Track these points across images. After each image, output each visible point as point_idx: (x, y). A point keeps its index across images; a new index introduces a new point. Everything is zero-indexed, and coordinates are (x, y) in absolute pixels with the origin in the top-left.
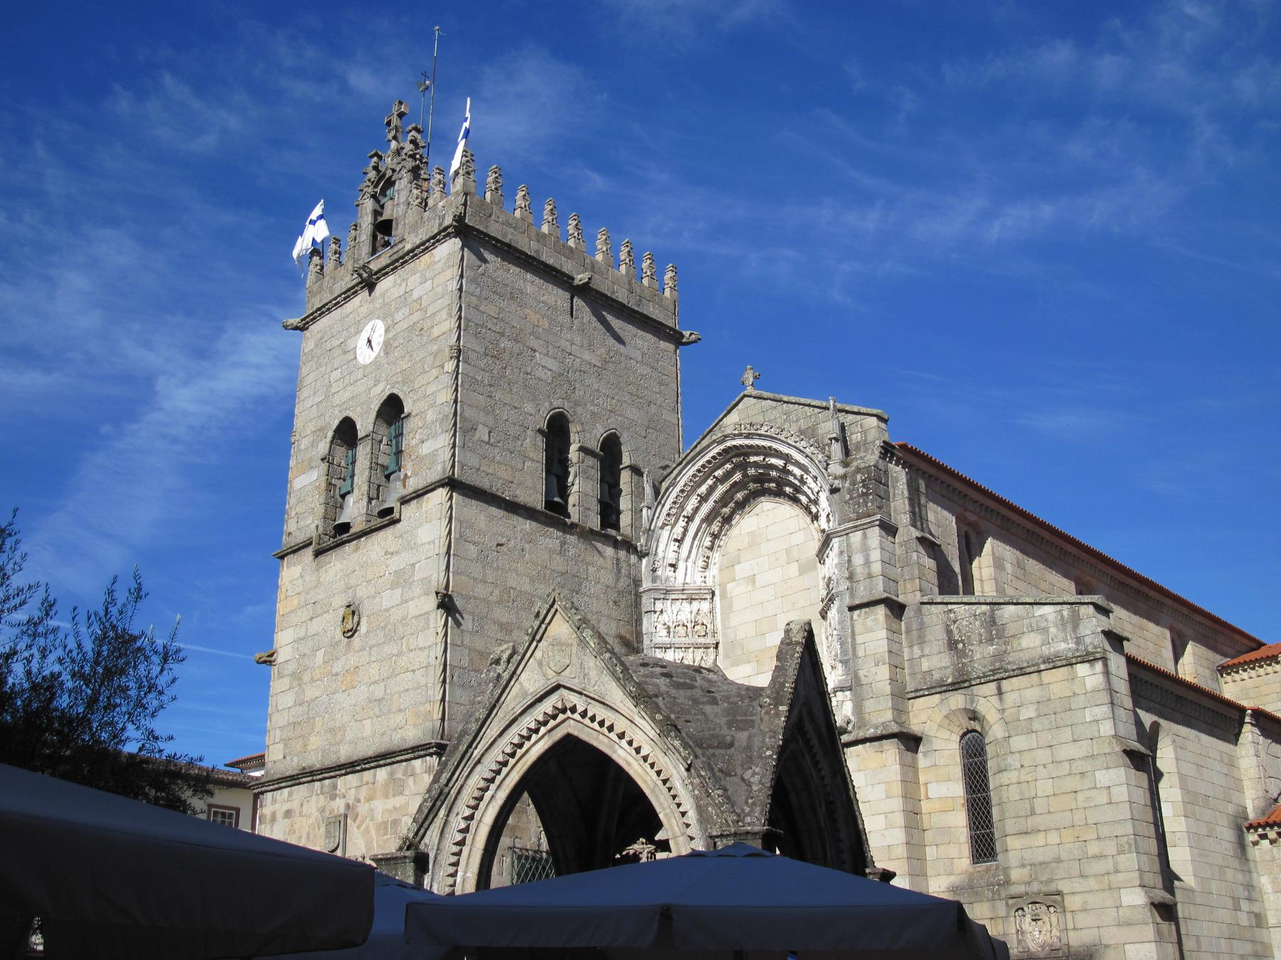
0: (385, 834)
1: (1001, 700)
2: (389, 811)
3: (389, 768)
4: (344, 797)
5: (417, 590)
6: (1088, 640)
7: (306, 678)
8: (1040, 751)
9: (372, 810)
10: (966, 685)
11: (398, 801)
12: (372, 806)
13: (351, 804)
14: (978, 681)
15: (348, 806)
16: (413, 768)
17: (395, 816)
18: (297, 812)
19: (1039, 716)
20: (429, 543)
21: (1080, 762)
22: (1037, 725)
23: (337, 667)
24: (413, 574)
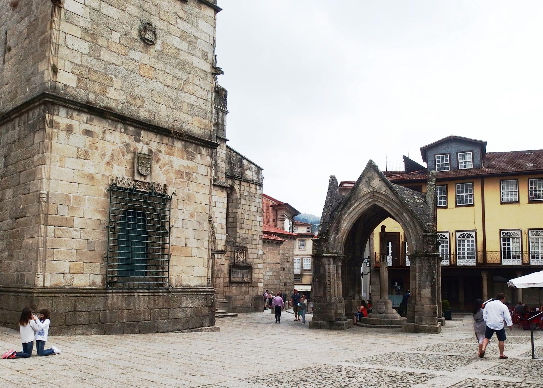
0: (182, 178)
1: (240, 187)
2: (184, 167)
3: (183, 143)
4: (147, 144)
5: (199, 55)
6: (260, 179)
7: (102, 42)
8: (247, 206)
9: (171, 161)
10: (234, 178)
11: (190, 164)
12: (171, 159)
13: (153, 151)
14: (236, 178)
15: (150, 151)
16: (200, 150)
17: (188, 170)
18: (100, 135)
19: (248, 196)
20: (206, 33)
21: (255, 213)
22: (247, 198)
23: (133, 55)
24: (196, 42)
